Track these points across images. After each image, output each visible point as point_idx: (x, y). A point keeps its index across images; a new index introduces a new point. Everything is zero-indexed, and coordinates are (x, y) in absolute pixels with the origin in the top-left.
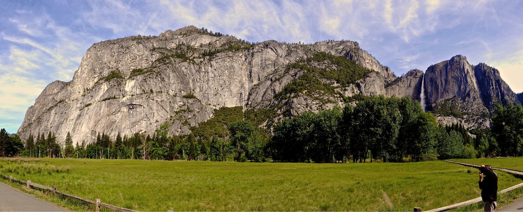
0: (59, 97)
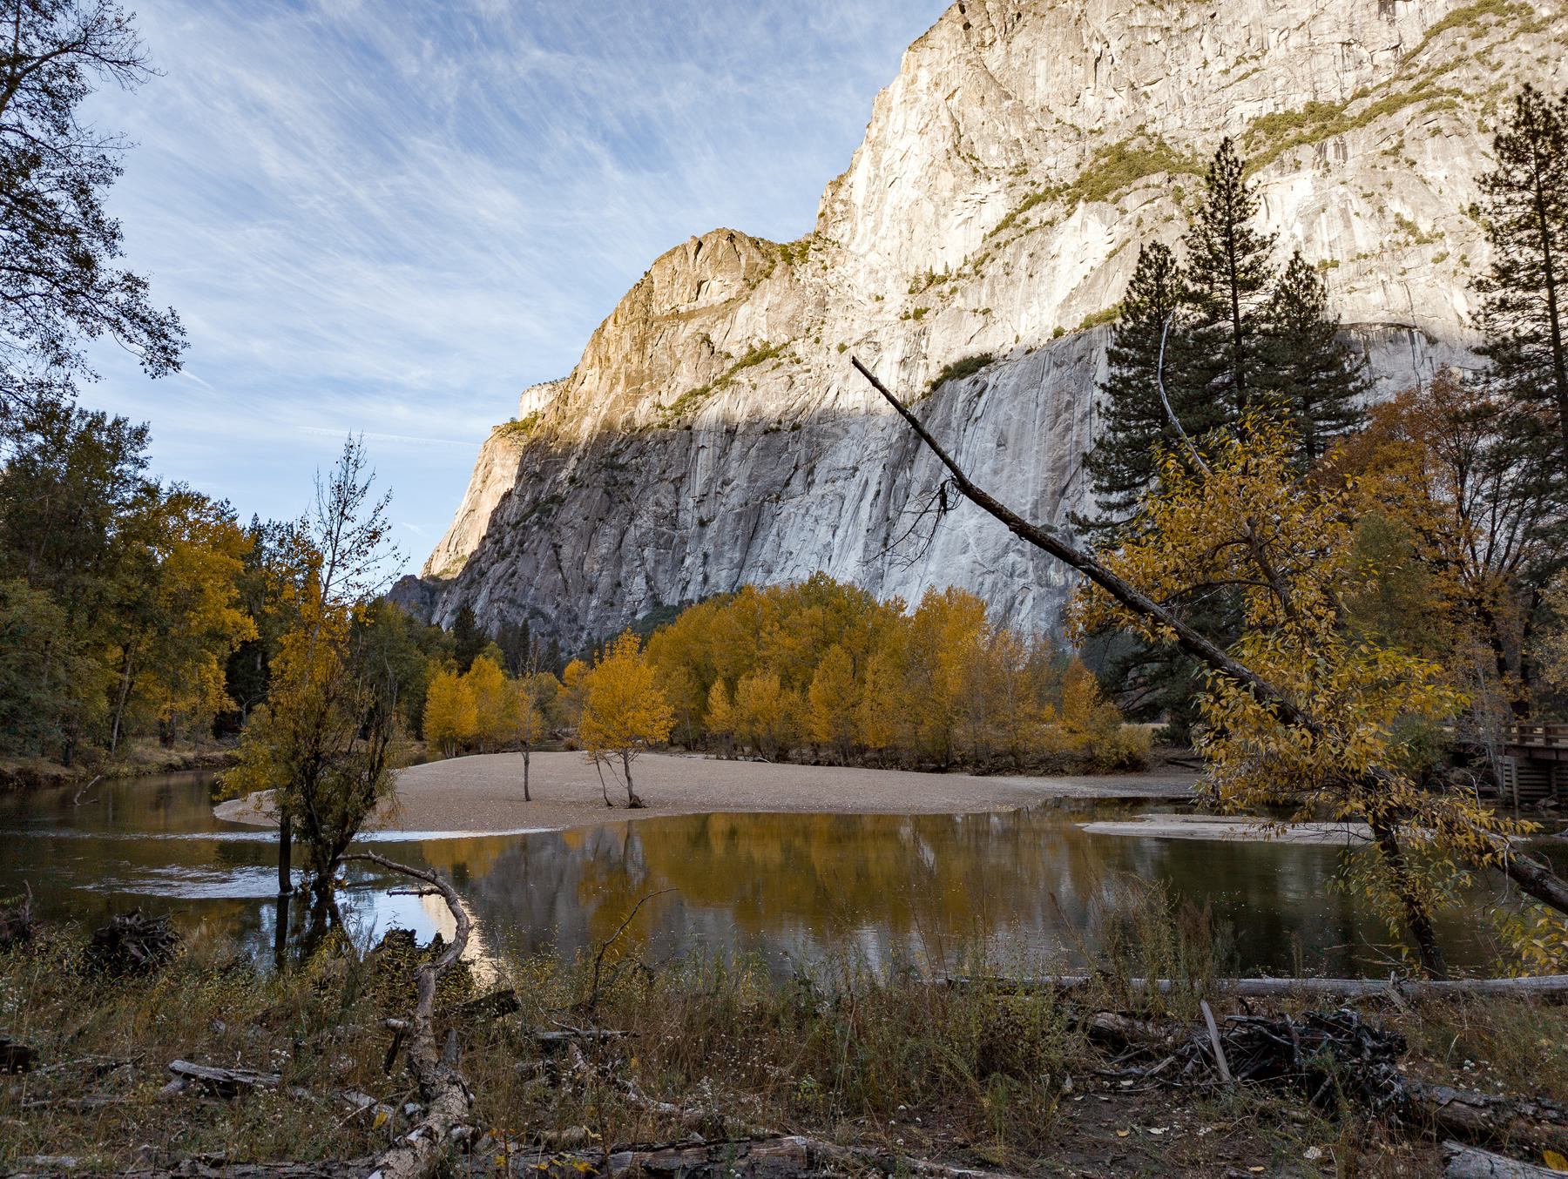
0: (739, 332)
